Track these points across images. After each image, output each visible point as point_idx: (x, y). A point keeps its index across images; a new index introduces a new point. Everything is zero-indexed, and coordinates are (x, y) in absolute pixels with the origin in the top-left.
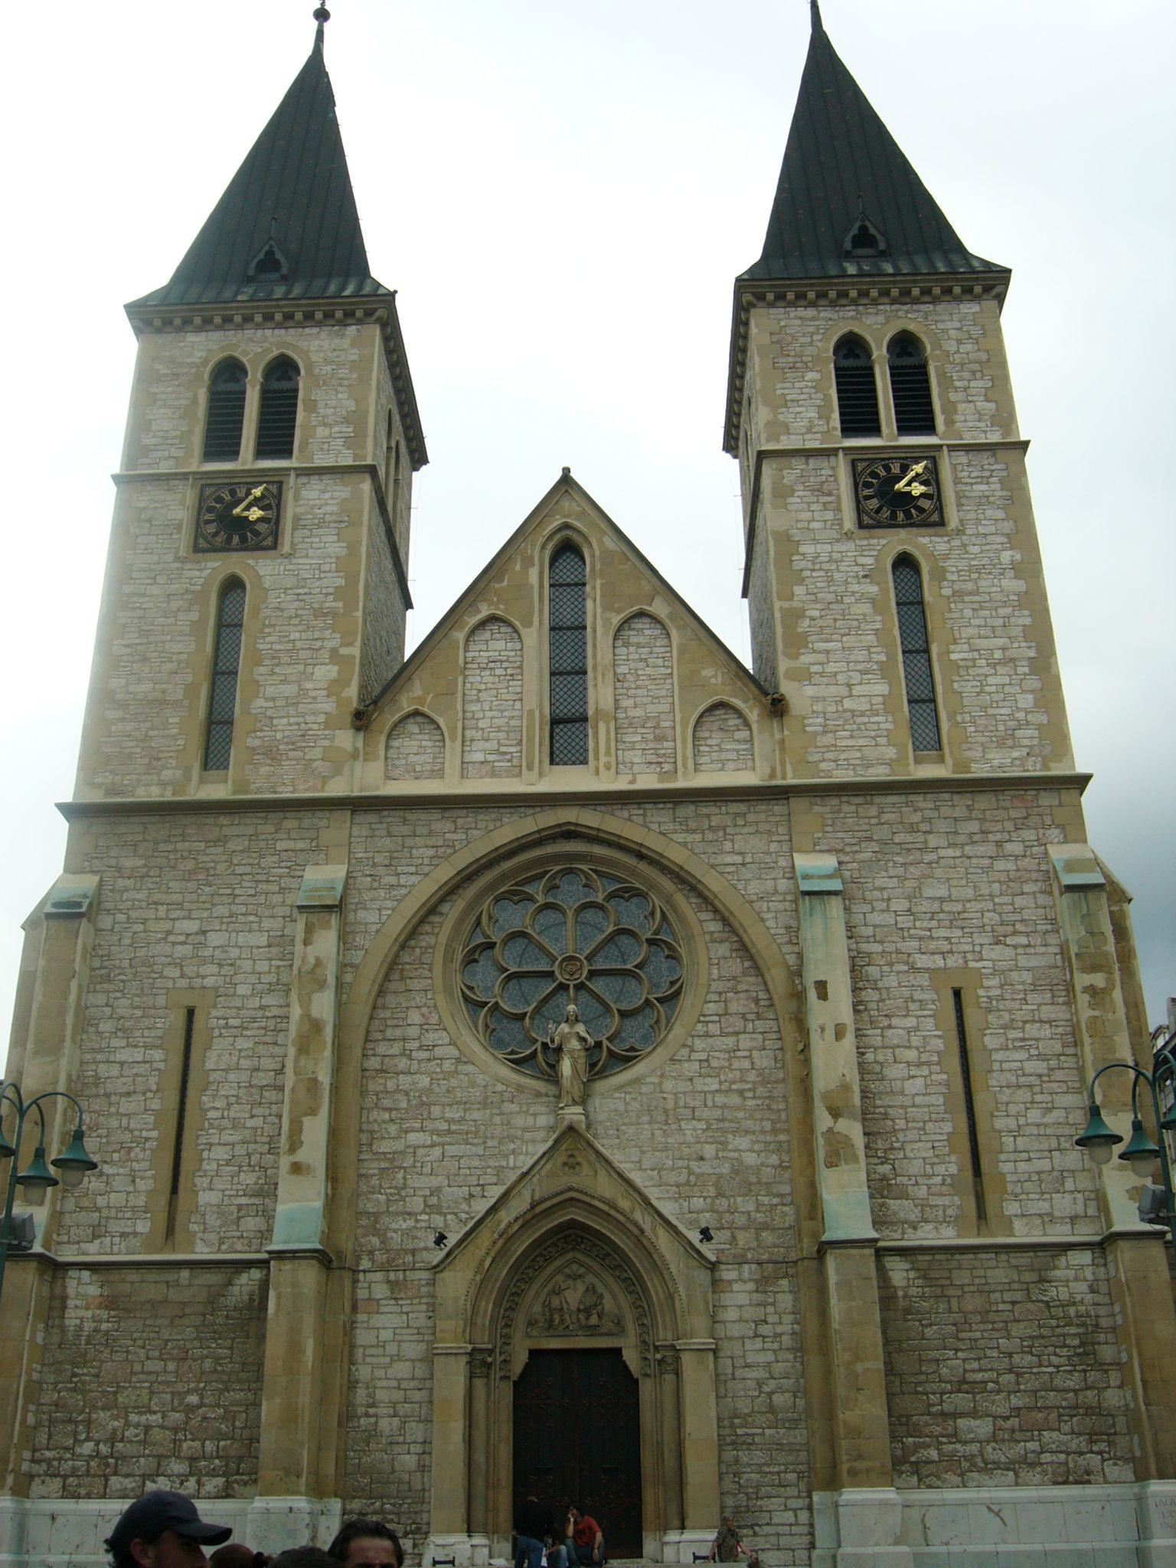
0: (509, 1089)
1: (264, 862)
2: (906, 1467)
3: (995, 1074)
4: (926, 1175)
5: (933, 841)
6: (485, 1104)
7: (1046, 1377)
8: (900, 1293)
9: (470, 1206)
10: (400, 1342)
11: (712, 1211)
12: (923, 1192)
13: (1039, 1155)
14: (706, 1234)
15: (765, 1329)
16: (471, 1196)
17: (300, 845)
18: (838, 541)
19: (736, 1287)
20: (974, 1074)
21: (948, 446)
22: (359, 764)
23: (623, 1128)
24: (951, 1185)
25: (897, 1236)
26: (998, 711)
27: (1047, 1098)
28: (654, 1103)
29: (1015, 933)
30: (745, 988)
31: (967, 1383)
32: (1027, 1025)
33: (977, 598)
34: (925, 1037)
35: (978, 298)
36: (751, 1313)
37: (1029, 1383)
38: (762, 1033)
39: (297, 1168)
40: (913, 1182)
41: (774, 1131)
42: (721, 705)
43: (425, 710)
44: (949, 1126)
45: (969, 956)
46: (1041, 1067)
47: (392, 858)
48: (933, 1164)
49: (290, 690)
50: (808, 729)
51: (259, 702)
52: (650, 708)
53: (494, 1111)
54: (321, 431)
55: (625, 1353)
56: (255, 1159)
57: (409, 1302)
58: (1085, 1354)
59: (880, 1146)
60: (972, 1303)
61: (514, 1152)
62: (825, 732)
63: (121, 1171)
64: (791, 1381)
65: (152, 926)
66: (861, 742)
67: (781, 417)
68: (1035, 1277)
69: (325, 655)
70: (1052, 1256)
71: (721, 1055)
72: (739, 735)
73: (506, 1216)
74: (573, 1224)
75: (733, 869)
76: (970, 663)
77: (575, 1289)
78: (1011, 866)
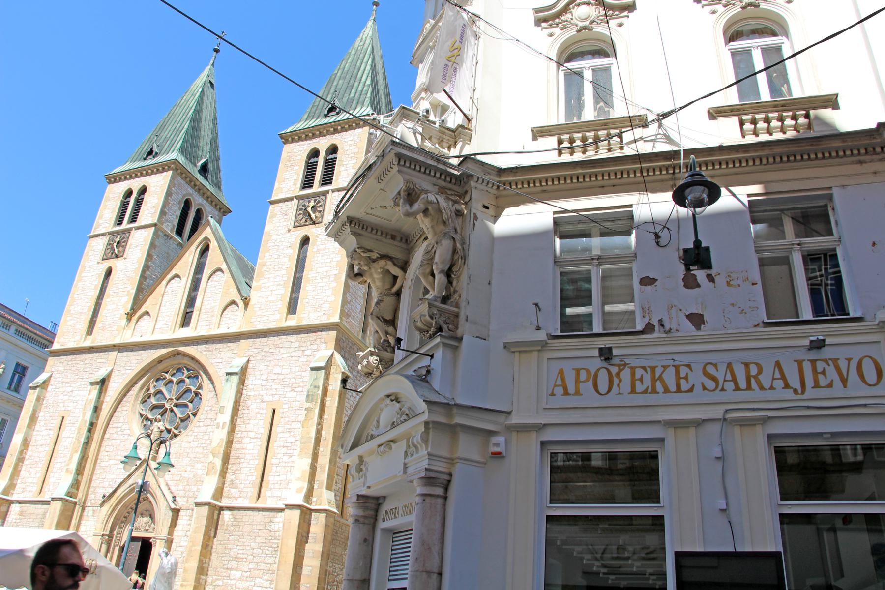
2: (211, 587)
3: (277, 442)
5: (282, 351)
7: (263, 558)
8: (226, 523)
11: (184, 490)
14: (174, 497)
17: (103, 360)
18: (285, 233)
21: (332, 190)
22: (125, 331)
24: (252, 484)
25: (230, 502)
27: (291, 452)
29: (299, 386)
32: (293, 423)
35: (362, 127)
36: (187, 528)
37: (257, 560)
42: (233, 303)
43: (148, 311)
46: (292, 439)
50: (255, 309)
51: (105, 311)
54: (146, 212)
65: (61, 389)
67: (281, 186)
72: (237, 313)
76: (314, 278)
78: (305, 360)
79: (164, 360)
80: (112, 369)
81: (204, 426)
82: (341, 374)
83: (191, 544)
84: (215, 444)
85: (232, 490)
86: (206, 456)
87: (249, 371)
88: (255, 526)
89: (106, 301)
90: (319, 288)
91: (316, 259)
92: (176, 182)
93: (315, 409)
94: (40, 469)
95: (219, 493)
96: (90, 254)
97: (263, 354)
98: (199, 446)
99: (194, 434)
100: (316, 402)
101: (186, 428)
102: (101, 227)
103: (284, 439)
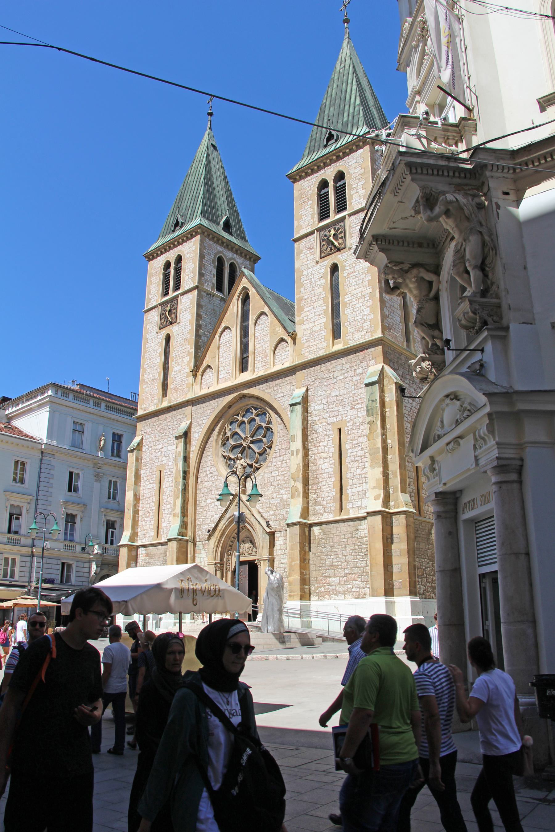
1: (174, 424)
5: (336, 374)
8: (317, 538)
12: (325, 503)
13: (359, 485)
14: (268, 522)
17: (182, 416)
19: (280, 539)
22: (194, 387)
25: (317, 519)
26: (358, 318)
29: (358, 403)
31: (333, 566)
33: (355, 274)
36: (283, 547)
42: (282, 340)
43: (209, 364)
45: (343, 416)
46: (362, 453)
47: (201, 415)
48: (328, 493)
49: (179, 367)
51: (173, 373)
52: (264, 346)
54: (187, 278)
59: (314, 488)
60: (336, 539)
62: (307, 342)
63: (149, 519)
66: (317, 342)
68: (354, 529)
69: (187, 353)
72: (287, 349)
73: (222, 523)
75: (281, 398)
76: (351, 301)
79: (233, 404)
80: (191, 422)
81: (280, 456)
82: (394, 384)
83: (290, 560)
84: (293, 470)
85: (317, 508)
86: (287, 482)
87: (310, 398)
88: (343, 536)
89: (172, 364)
90: (357, 309)
91: (348, 283)
92: (205, 245)
93: (377, 421)
94: (152, 517)
95: (305, 512)
96: (148, 327)
97: (319, 381)
99: (273, 464)
100: (377, 415)
101: (265, 460)
102: (151, 301)
103: (354, 454)
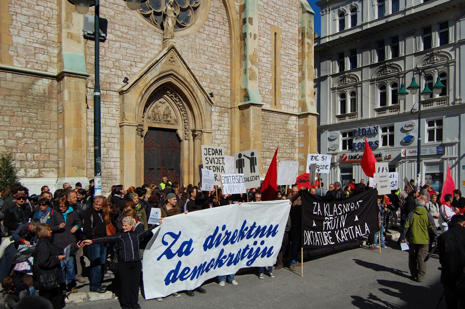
0: (145, 26)
4: (265, 88)
6: (136, 29)
9: (131, 69)
10: (106, 119)
13: (288, 88)
15: (221, 128)
16: (131, 65)
19: (214, 114)
20: (277, 60)
23: (183, 52)
27: (291, 72)
28: (193, 46)
30: (220, 13)
34: (268, 45)
36: (217, 123)
38: (225, 30)
39: (71, 36)
40: (262, 89)
41: (226, 65)
44: (270, 75)
53: (139, 33)
55: (178, 131)
56: (41, 26)
57: (109, 103)
58: (292, 144)
61: (147, 51)
64: (227, 145)
68: (285, 122)
70: (289, 117)
71: (213, 34)
74: (169, 84)
77: (162, 107)
88: (277, 126)
98: (213, 46)
